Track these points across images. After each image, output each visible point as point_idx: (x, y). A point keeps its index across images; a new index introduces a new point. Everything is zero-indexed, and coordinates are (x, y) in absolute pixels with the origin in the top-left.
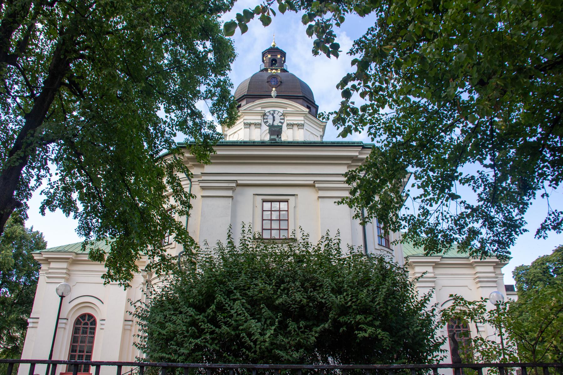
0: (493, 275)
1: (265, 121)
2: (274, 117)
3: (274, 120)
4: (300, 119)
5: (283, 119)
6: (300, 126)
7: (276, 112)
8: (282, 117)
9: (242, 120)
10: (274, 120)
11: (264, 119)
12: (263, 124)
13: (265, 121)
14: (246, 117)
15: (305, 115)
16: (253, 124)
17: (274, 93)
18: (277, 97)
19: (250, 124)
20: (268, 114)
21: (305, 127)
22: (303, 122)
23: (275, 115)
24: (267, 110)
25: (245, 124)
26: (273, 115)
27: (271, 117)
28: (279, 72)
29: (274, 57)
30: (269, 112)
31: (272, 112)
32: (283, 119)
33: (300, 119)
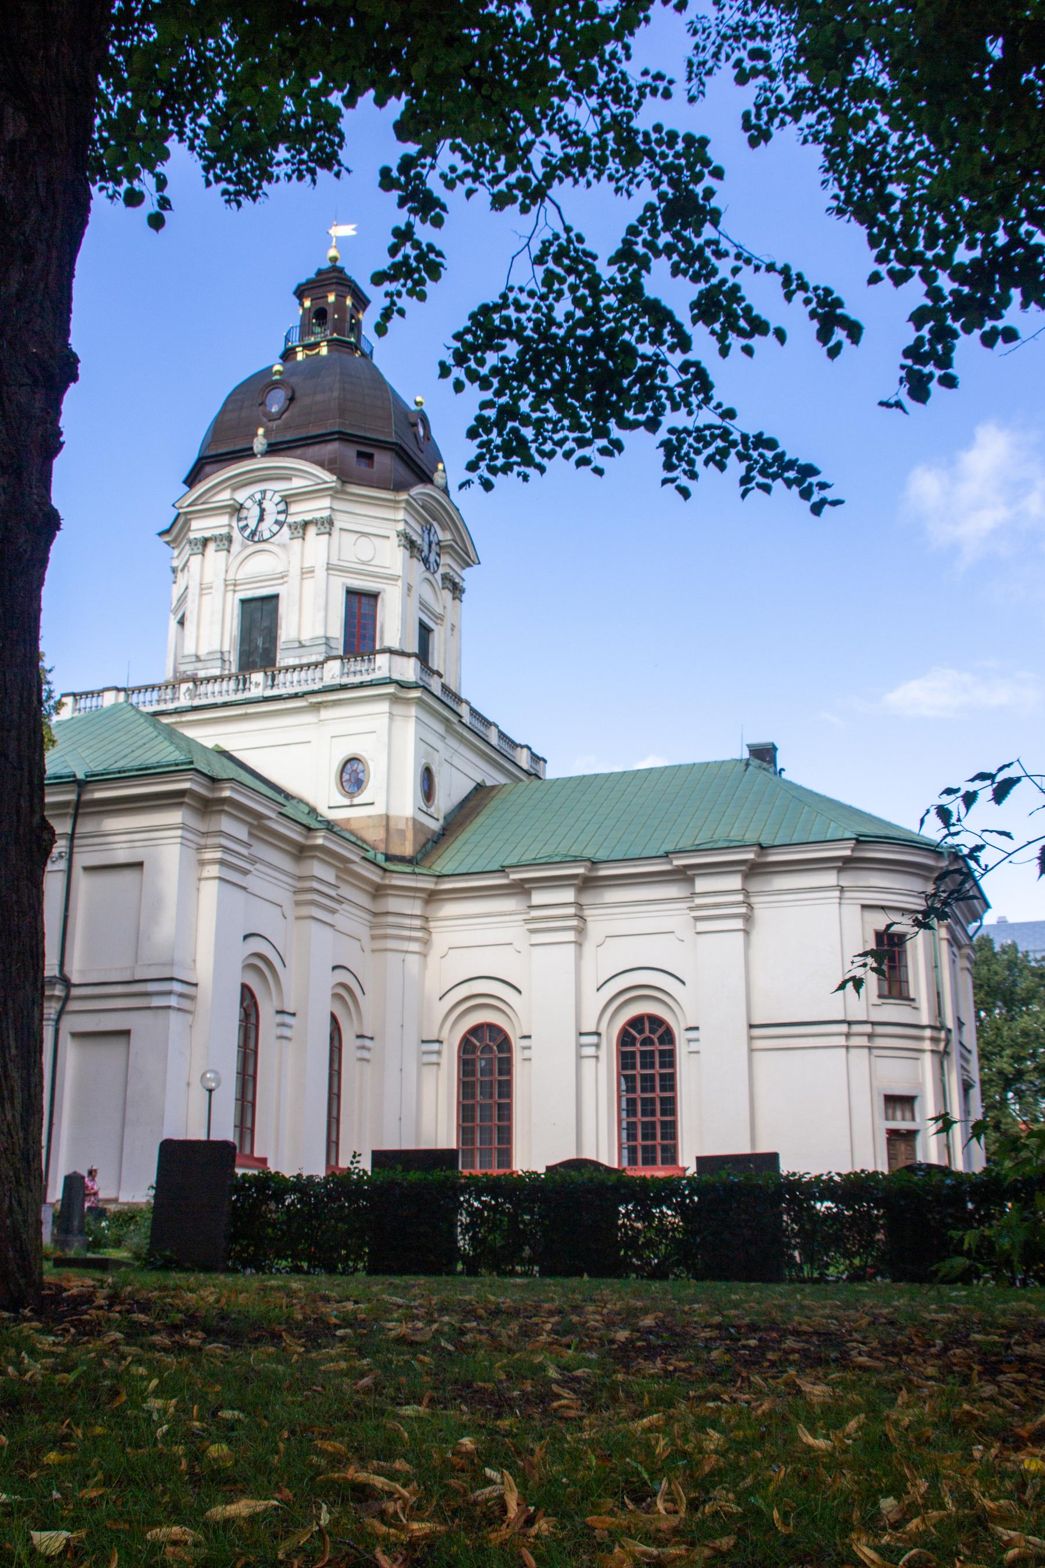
1: (242, 524)
2: (262, 511)
3: (261, 519)
4: (318, 507)
5: (285, 512)
7: (269, 495)
8: (282, 507)
10: (261, 519)
11: (239, 520)
13: (242, 524)
15: (335, 494)
16: (214, 539)
17: (259, 443)
18: (274, 449)
20: (249, 504)
21: (338, 525)
22: (326, 514)
23: (266, 504)
24: (241, 496)
26: (260, 504)
27: (256, 511)
28: (324, 351)
29: (320, 304)
31: (258, 496)
32: (285, 512)
33: (318, 507)
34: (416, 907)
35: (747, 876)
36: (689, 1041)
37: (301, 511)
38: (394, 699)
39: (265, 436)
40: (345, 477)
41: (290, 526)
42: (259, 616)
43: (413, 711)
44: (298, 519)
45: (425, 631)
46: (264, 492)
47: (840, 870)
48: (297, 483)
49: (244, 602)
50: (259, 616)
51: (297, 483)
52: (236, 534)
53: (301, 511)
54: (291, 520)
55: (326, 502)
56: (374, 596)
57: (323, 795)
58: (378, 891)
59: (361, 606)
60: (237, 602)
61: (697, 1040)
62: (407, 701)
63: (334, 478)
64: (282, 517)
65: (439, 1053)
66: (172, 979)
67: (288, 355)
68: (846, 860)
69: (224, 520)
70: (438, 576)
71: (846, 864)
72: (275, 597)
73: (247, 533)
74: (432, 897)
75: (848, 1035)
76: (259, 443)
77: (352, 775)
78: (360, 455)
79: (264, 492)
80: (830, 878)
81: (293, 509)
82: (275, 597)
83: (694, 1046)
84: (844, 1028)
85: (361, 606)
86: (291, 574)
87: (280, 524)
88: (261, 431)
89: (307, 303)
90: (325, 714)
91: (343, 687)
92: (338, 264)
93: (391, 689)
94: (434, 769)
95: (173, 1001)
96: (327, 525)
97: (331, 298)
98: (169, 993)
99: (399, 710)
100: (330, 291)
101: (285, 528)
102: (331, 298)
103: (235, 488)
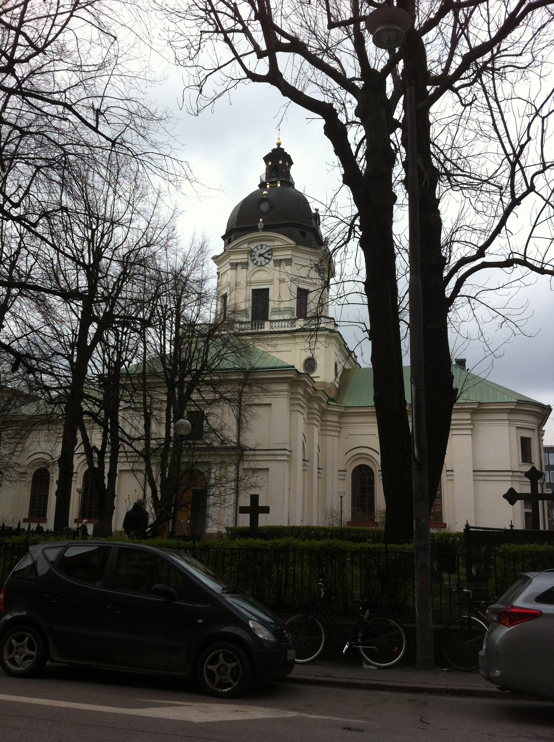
0: (470, 422)
1: (253, 258)
6: (289, 262)
9: (228, 260)
11: (251, 256)
12: (250, 262)
13: (253, 258)
14: (232, 257)
15: (293, 249)
17: (260, 225)
18: (266, 228)
19: (237, 264)
21: (294, 262)
22: (290, 257)
24: (253, 246)
25: (231, 264)
28: (279, 185)
30: (257, 247)
34: (336, 419)
35: (472, 414)
36: (448, 475)
37: (278, 255)
39: (263, 222)
40: (298, 243)
41: (274, 261)
42: (260, 297)
44: (278, 258)
46: (262, 246)
47: (509, 413)
48: (277, 243)
49: (253, 290)
50: (260, 297)
51: (277, 243)
52: (250, 262)
53: (278, 255)
54: (273, 258)
55: (290, 252)
56: (307, 292)
60: (251, 291)
61: (453, 475)
63: (294, 243)
64: (270, 257)
65: (344, 475)
66: (286, 449)
68: (511, 409)
69: (245, 256)
71: (511, 411)
72: (268, 289)
73: (255, 262)
74: (342, 415)
75: (512, 476)
76: (260, 225)
78: (301, 232)
79: (262, 246)
80: (505, 416)
81: (275, 254)
82: (268, 289)
83: (450, 478)
84: (511, 474)
86: (275, 280)
88: (261, 220)
89: (270, 163)
92: (281, 146)
93: (327, 332)
97: (281, 162)
98: (285, 455)
99: (328, 341)
100: (280, 160)
101: (272, 262)
102: (281, 162)
103: (249, 243)
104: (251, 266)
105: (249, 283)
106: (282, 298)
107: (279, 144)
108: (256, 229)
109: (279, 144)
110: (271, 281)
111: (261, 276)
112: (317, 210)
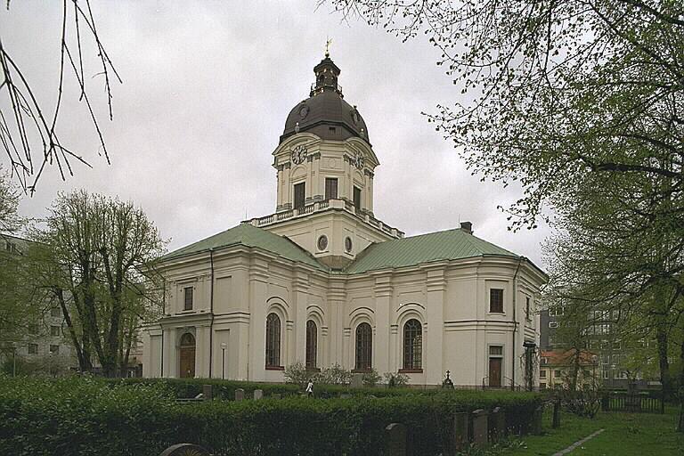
6: (318, 155)
15: (320, 144)
37: (311, 151)
38: (335, 215)
42: (300, 188)
43: (342, 219)
45: (357, 192)
50: (300, 188)
57: (313, 248)
58: (328, 281)
59: (331, 184)
62: (339, 216)
67: (312, 94)
70: (363, 171)
71: (480, 265)
77: (322, 242)
80: (474, 270)
85: (331, 184)
87: (305, 157)
90: (314, 222)
91: (319, 212)
93: (333, 212)
94: (352, 239)
95: (241, 320)
96: (318, 155)
104: (293, 165)
105: (292, 180)
106: (315, 189)
107: (327, 55)
108: (294, 133)
109: (327, 55)
110: (304, 177)
111: (299, 173)
112: (355, 107)
